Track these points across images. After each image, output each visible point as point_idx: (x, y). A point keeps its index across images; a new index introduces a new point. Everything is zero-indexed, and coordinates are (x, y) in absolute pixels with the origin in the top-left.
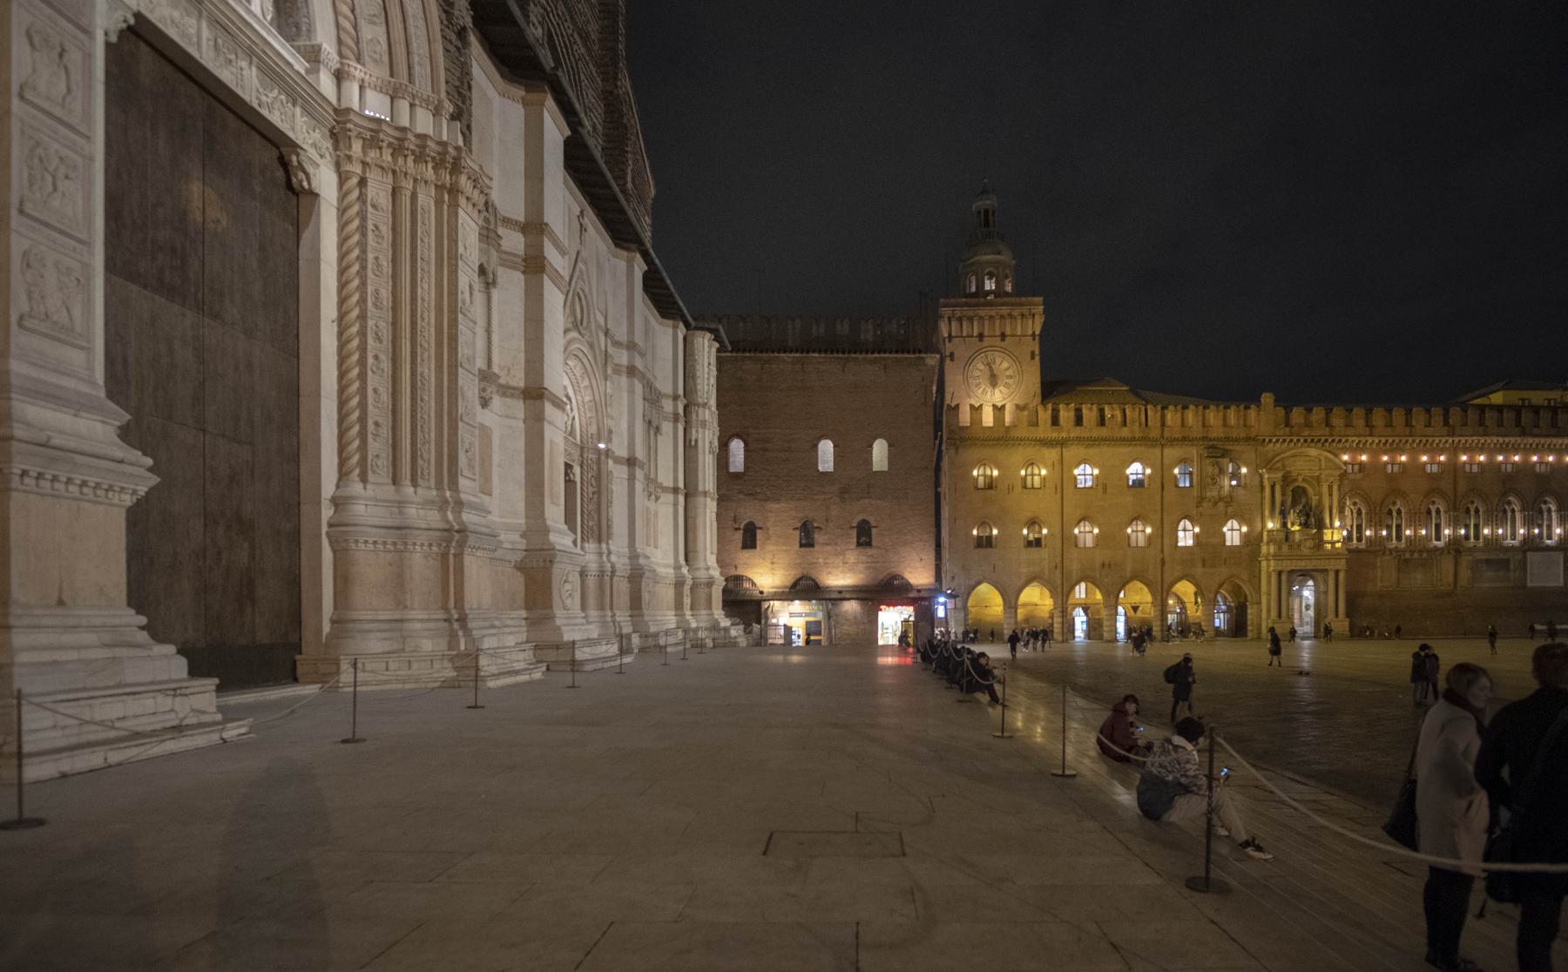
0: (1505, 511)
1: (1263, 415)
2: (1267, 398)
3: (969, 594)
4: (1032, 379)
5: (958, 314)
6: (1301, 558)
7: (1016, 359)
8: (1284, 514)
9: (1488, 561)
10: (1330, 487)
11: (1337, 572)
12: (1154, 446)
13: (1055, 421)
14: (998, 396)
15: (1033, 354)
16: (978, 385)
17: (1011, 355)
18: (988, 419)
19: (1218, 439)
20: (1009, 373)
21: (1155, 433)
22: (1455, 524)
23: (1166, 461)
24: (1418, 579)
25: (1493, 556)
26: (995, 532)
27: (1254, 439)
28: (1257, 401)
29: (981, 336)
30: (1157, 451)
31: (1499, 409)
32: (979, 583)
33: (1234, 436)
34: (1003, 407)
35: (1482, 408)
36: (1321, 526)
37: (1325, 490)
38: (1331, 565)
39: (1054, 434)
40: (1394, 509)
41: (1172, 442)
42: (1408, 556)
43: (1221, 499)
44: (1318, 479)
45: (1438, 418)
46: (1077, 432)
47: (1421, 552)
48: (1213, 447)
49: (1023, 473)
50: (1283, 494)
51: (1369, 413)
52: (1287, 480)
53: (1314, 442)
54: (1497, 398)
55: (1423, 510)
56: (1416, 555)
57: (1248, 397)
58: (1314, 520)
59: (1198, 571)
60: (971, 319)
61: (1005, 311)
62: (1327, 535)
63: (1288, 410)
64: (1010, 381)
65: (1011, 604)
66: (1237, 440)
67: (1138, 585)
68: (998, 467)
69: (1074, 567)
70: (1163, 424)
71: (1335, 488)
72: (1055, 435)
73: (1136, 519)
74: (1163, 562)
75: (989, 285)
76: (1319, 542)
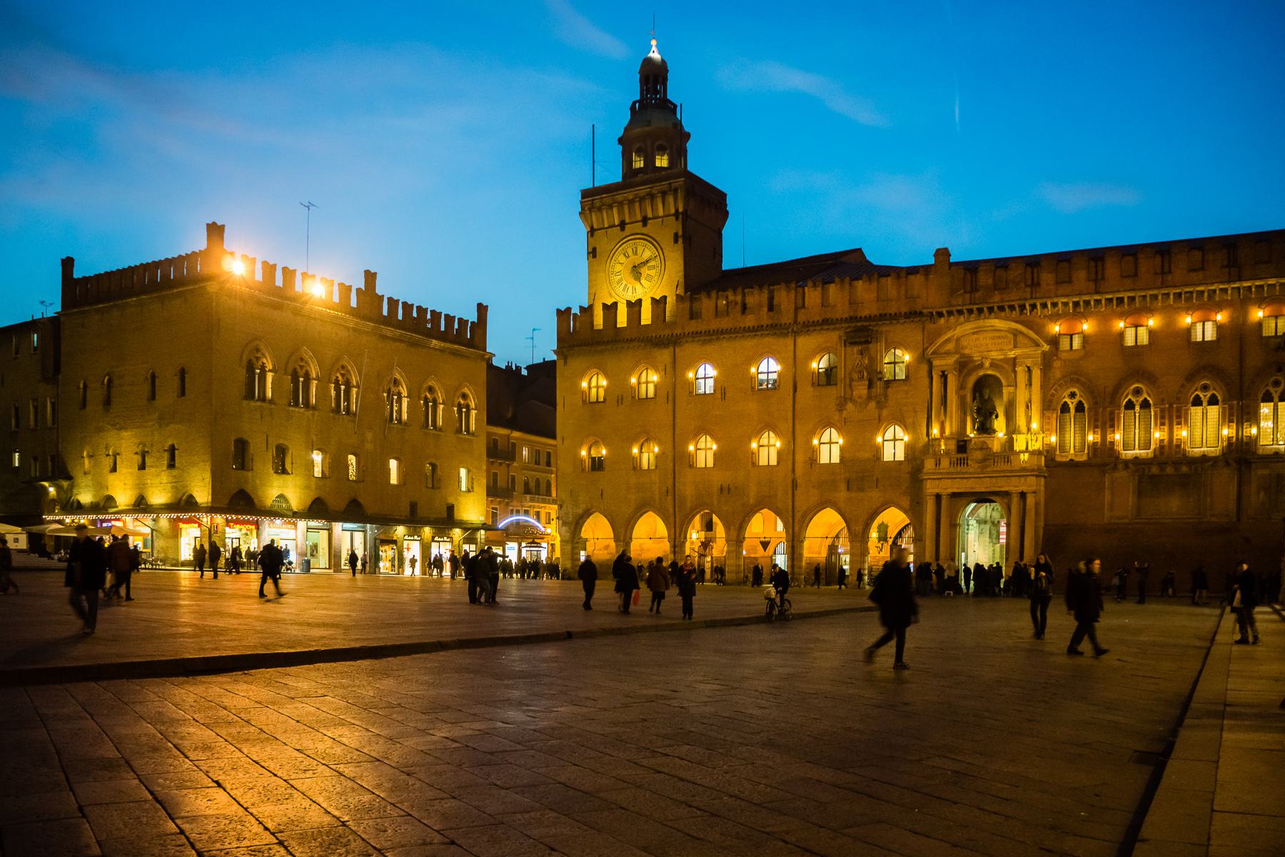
12: (786, 335)
13: (693, 315)
15: (676, 236)
16: (619, 282)
19: (869, 318)
21: (787, 318)
23: (800, 354)
29: (622, 225)
30: (789, 341)
33: (893, 310)
34: (615, 304)
38: (1014, 486)
41: (809, 327)
50: (961, 387)
52: (964, 366)
59: (842, 495)
64: (652, 272)
66: (893, 318)
69: (688, 490)
71: (1037, 374)
74: (794, 485)
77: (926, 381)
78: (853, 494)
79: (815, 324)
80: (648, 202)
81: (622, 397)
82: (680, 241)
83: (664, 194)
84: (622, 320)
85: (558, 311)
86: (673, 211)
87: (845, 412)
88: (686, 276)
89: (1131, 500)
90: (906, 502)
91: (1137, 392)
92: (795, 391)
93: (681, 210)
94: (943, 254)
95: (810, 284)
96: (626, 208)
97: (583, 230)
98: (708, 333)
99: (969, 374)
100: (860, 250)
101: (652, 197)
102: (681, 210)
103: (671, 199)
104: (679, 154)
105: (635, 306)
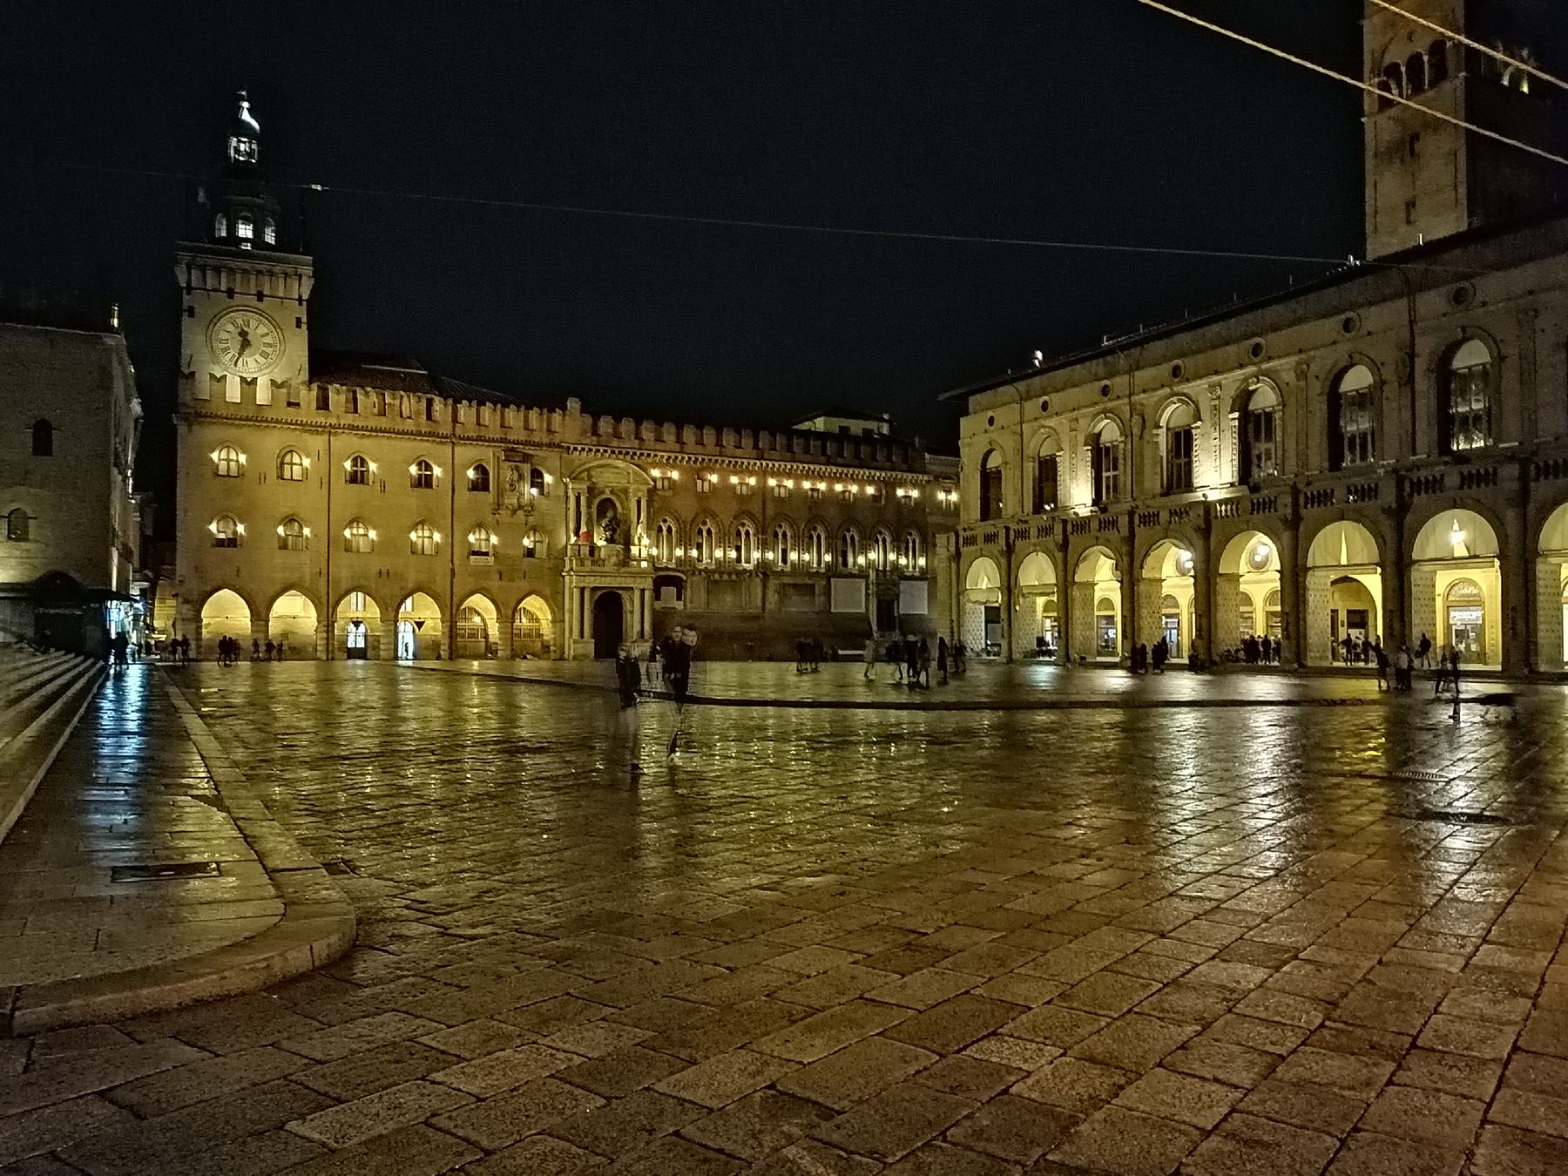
0: (811, 538)
1: (569, 422)
2: (573, 404)
3: (203, 602)
4: (298, 349)
6: (604, 575)
7: (276, 326)
9: (795, 586)
10: (639, 502)
11: (643, 591)
13: (323, 404)
14: (251, 365)
15: (299, 323)
16: (226, 350)
18: (233, 393)
19: (518, 443)
20: (267, 340)
21: (446, 429)
22: (764, 546)
24: (727, 602)
25: (799, 581)
28: (564, 409)
30: (448, 449)
31: (823, 436)
32: (219, 589)
33: (537, 440)
35: (808, 435)
36: (628, 543)
37: (633, 505)
39: (320, 418)
43: (520, 507)
44: (626, 491)
45: (747, 441)
46: (349, 419)
47: (730, 574)
48: (513, 450)
50: (589, 507)
51: (679, 428)
53: (622, 453)
54: (820, 424)
55: (733, 531)
56: (725, 577)
57: (551, 401)
58: (621, 534)
59: (494, 584)
61: (264, 266)
62: (634, 550)
63: (596, 418)
65: (260, 616)
66: (540, 445)
67: (419, 596)
70: (455, 420)
73: (422, 523)
74: (453, 570)
75: (245, 231)
76: (626, 559)
78: (504, 583)
82: (304, 327)
89: (703, 595)
90: (547, 591)
93: (305, 297)
101: (271, 274)
102: (305, 297)
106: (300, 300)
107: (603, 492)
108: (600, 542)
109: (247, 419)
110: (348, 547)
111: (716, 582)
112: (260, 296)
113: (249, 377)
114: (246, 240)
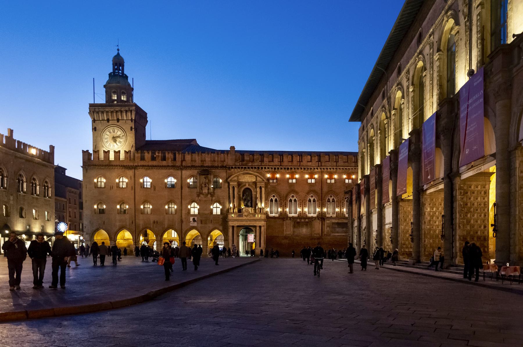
5: (97, 110)
8: (240, 199)
9: (338, 224)
10: (261, 188)
15: (131, 128)
17: (121, 128)
19: (208, 167)
21: (178, 164)
23: (184, 177)
24: (304, 231)
25: (340, 221)
26: (95, 207)
27: (226, 167)
29: (108, 120)
30: (179, 172)
33: (216, 165)
40: (293, 199)
41: (186, 168)
42: (298, 220)
49: (117, 181)
50: (239, 192)
60: (103, 112)
64: (121, 140)
66: (217, 167)
68: (105, 178)
72: (131, 164)
74: (182, 221)
77: (228, 189)
78: (203, 225)
79: (188, 167)
80: (119, 113)
81: (111, 186)
82: (133, 130)
83: (126, 111)
84: (112, 157)
85: (83, 151)
86: (130, 118)
87: (200, 198)
88: (136, 143)
90: (221, 228)
91: (293, 197)
92: (182, 189)
93: (133, 118)
94: (233, 148)
95: (187, 153)
96: (110, 114)
97: (90, 120)
98: (148, 166)
99: (241, 188)
100: (195, 140)
102: (133, 118)
103: (129, 114)
104: (130, 96)
105: (117, 153)
106: (132, 120)
107: (245, 185)
108: (243, 207)
109: (106, 166)
110: (142, 212)
111: (298, 223)
112: (118, 120)
113: (117, 151)
114: (115, 100)
